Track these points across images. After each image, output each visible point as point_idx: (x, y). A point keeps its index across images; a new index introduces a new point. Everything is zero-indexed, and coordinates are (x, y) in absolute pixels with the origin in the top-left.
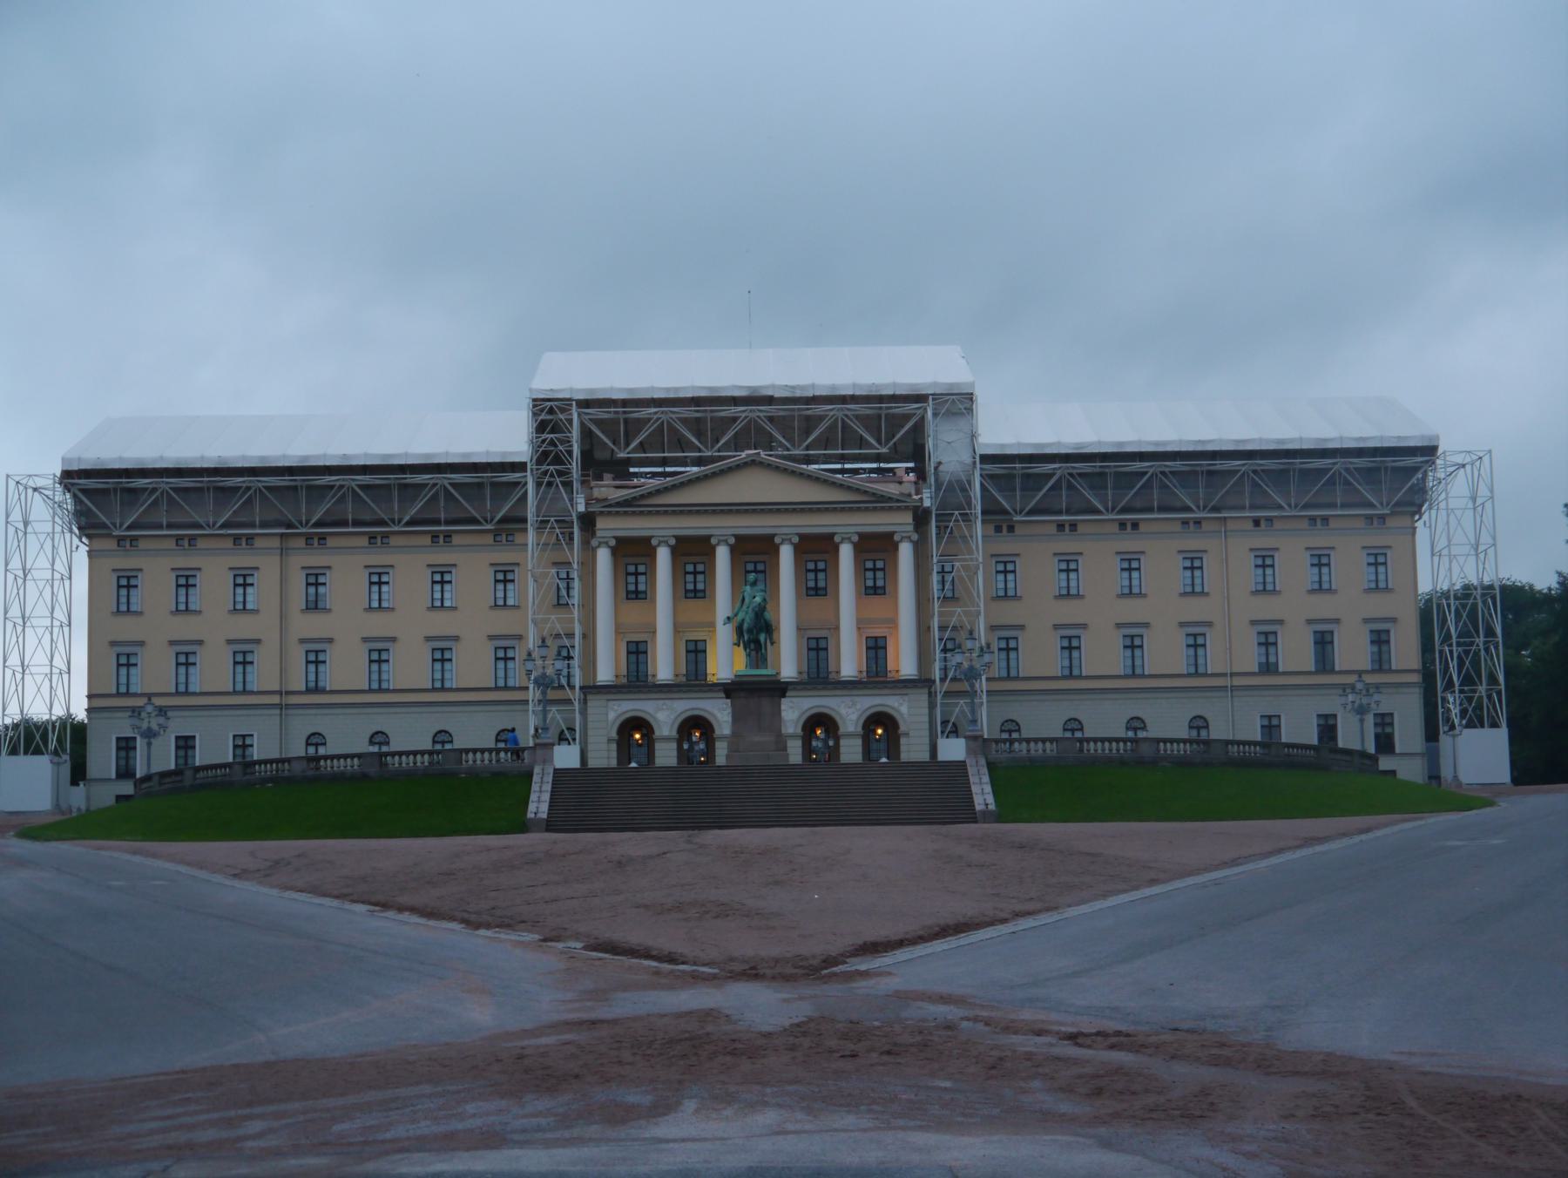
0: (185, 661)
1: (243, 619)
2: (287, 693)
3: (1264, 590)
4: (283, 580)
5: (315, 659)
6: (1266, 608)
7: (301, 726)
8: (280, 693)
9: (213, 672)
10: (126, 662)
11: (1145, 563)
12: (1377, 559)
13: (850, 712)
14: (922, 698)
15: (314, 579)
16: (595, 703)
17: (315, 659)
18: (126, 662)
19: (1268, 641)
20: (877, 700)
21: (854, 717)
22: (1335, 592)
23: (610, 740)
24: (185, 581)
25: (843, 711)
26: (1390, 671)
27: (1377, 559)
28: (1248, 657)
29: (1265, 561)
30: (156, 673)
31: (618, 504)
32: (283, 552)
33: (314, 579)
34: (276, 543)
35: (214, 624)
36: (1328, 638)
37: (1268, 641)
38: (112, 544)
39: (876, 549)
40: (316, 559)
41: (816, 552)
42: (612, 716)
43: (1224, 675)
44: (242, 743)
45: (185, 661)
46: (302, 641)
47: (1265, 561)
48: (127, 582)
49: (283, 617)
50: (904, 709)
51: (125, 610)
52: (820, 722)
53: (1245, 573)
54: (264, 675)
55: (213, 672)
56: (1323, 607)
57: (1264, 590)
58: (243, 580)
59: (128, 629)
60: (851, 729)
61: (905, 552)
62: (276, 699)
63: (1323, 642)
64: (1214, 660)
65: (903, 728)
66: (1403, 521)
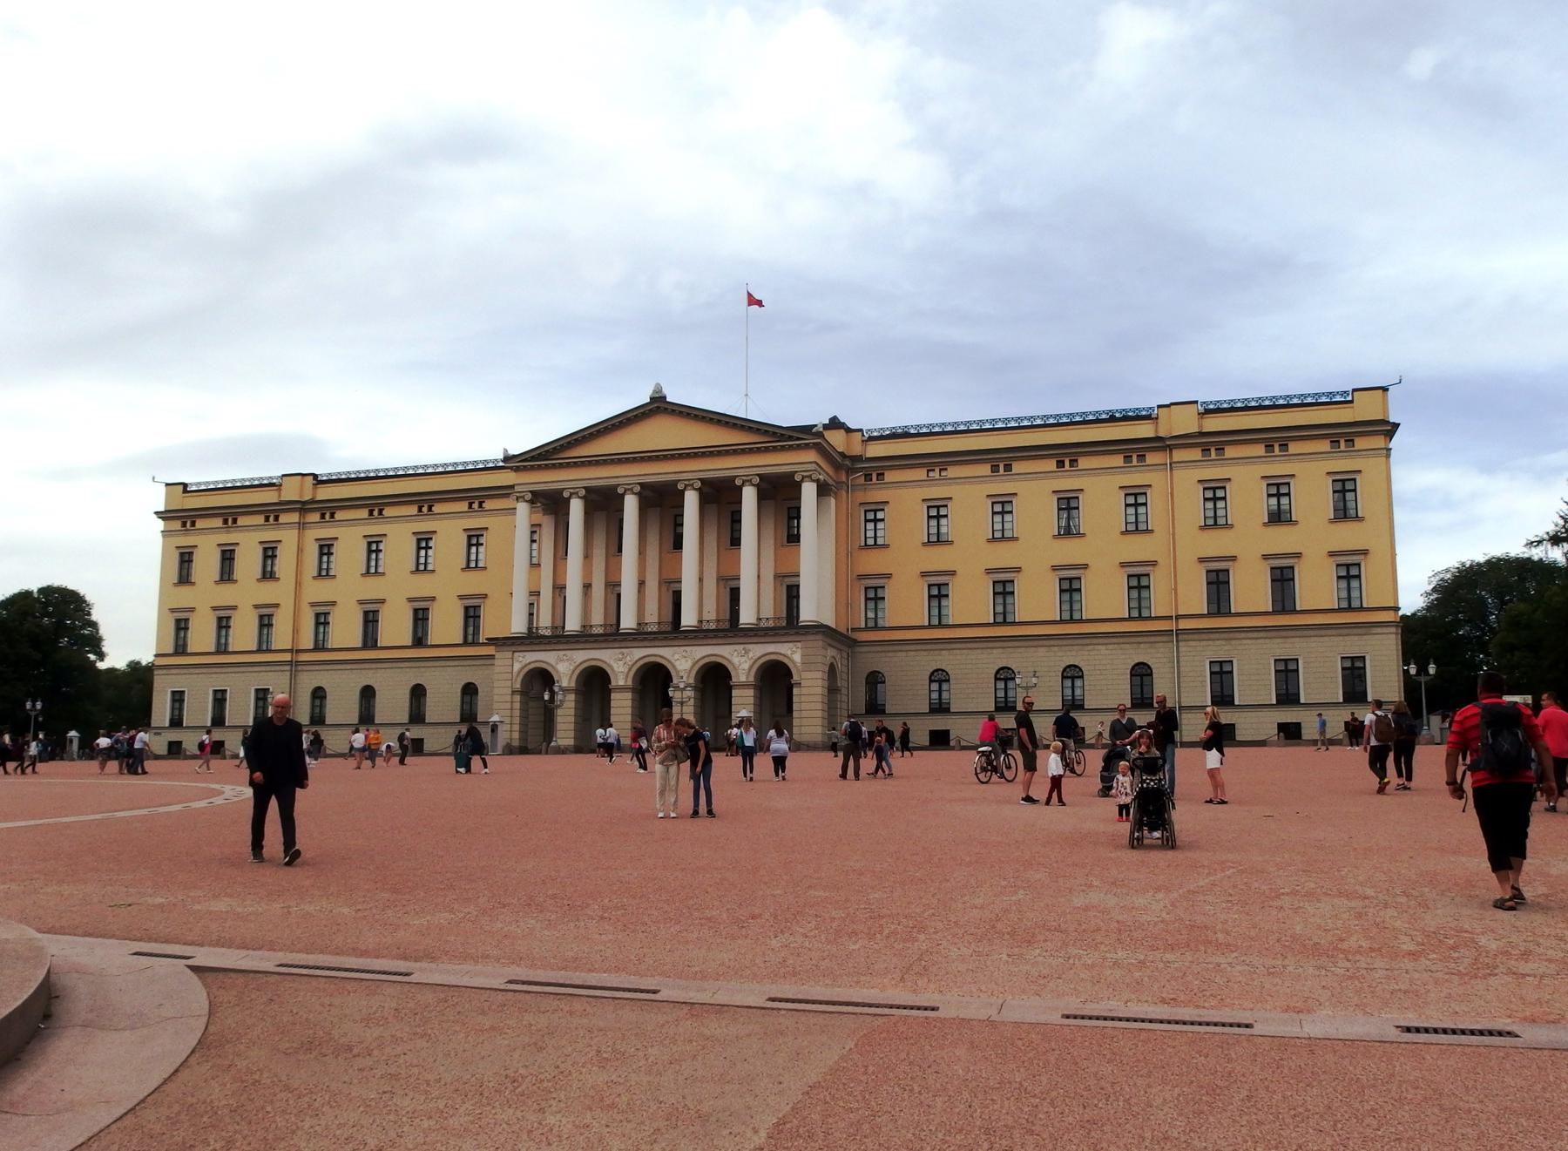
0: (223, 624)
1: (269, 586)
2: (298, 651)
3: (1214, 523)
4: (300, 550)
5: (322, 621)
6: (1216, 544)
7: (308, 681)
8: (291, 651)
9: (244, 634)
10: (181, 626)
11: (1084, 501)
12: (1344, 488)
13: (742, 661)
14: (817, 642)
15: (326, 549)
16: (502, 657)
17: (322, 621)
18: (181, 626)
19: (1218, 584)
20: (771, 648)
21: (746, 666)
22: (1296, 523)
23: (513, 692)
24: (228, 557)
25: (736, 660)
26: (1361, 609)
27: (1344, 488)
28: (1195, 598)
29: (1215, 493)
30: (202, 636)
31: (533, 459)
32: (302, 526)
33: (326, 549)
34: (295, 517)
35: (247, 592)
36: (1287, 574)
37: (1218, 584)
38: (177, 525)
39: (780, 496)
40: (326, 532)
41: (720, 498)
42: (517, 667)
44: (262, 695)
45: (223, 624)
46: (313, 605)
47: (1215, 493)
48: (186, 559)
49: (298, 584)
50: (797, 658)
51: (184, 578)
52: (714, 679)
53: (1192, 505)
54: (281, 637)
55: (244, 634)
56: (1282, 540)
57: (1214, 523)
58: (269, 553)
59: (185, 597)
60: (743, 679)
61: (809, 491)
62: (287, 657)
63: (1283, 579)
64: (1159, 602)
65: (796, 678)
66: (1379, 442)
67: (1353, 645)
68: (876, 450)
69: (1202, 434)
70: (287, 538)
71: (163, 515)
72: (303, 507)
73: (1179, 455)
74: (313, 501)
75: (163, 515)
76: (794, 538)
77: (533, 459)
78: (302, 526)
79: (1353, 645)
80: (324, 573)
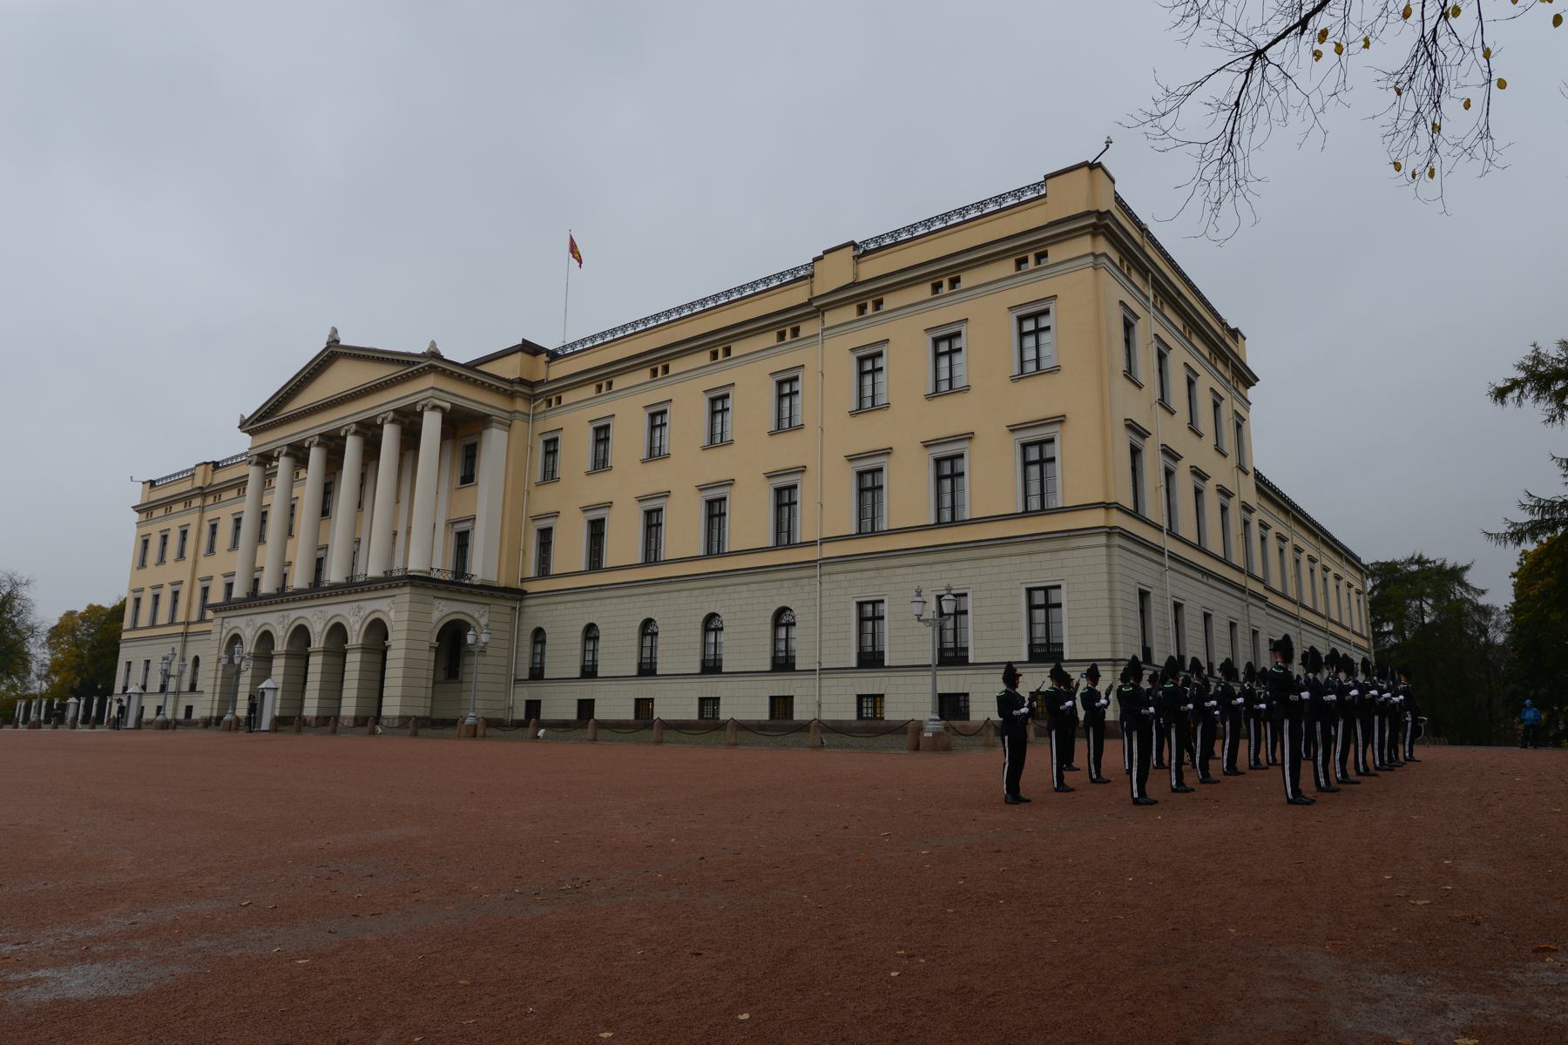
4: (200, 531)
21: (357, 627)
43: (813, 543)
49: (195, 562)
67: (1040, 568)
68: (560, 370)
69: (853, 285)
70: (192, 519)
71: (139, 509)
72: (203, 492)
73: (832, 318)
74: (210, 485)
75: (139, 509)
76: (468, 478)
77: (258, 420)
78: (202, 509)
79: (1040, 568)
80: (211, 549)
